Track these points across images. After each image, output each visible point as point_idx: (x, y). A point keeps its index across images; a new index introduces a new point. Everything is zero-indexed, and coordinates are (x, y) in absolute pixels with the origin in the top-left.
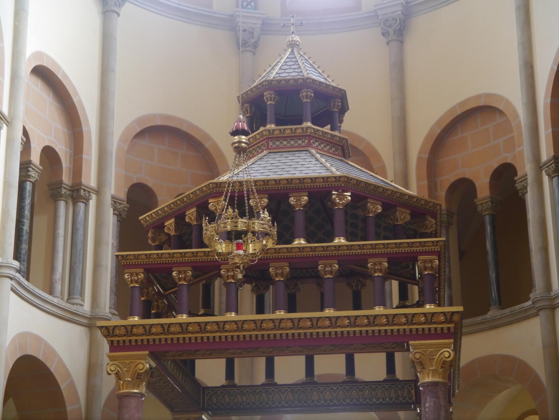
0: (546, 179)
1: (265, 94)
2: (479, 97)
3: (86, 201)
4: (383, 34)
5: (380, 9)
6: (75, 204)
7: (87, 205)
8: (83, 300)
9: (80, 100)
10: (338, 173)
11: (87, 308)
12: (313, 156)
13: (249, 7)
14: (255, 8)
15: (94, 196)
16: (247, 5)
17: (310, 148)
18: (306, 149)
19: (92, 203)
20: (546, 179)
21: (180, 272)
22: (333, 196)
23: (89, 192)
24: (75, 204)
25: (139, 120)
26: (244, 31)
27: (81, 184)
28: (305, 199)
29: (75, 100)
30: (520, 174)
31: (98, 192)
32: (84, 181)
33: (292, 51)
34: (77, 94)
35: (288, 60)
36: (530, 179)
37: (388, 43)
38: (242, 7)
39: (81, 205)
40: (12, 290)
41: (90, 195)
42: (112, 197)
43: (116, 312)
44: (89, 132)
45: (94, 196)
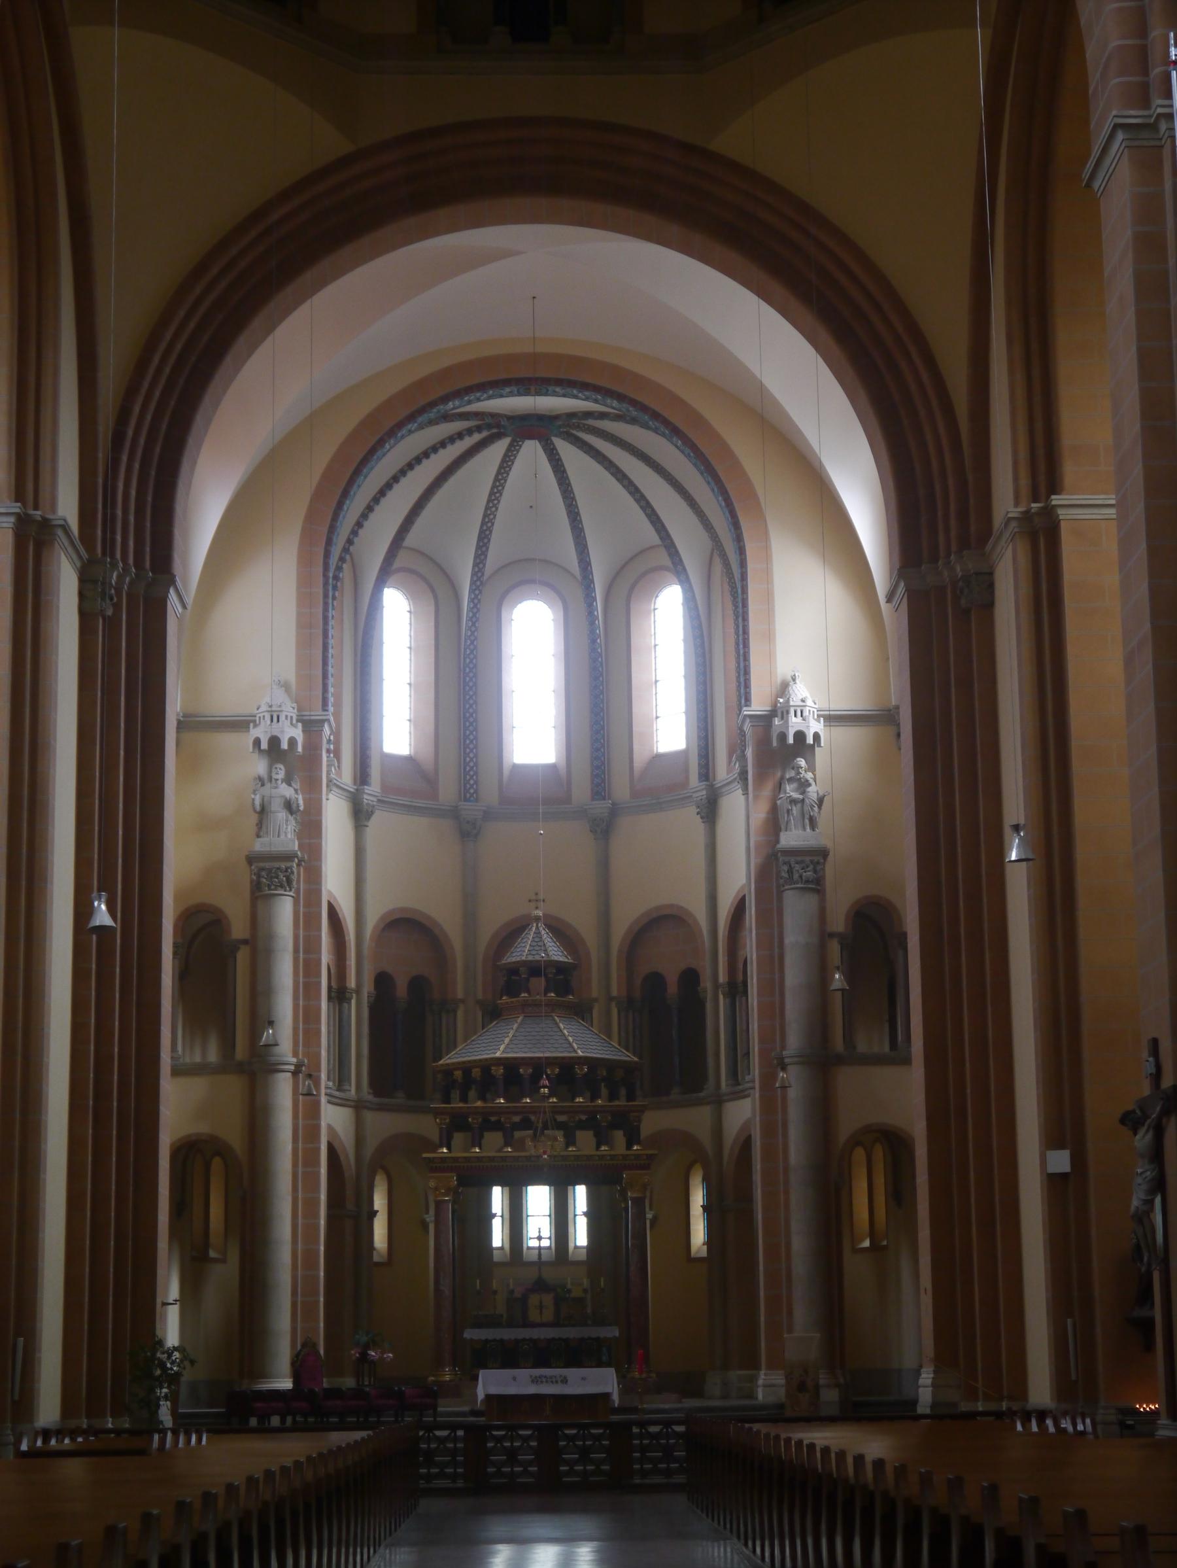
0: (721, 997)
1: (521, 969)
2: (672, 906)
3: (349, 1001)
4: (591, 831)
5: (590, 808)
6: (340, 1004)
7: (350, 1004)
8: (350, 1085)
9: (343, 914)
10: (580, 1053)
11: (353, 1092)
12: (556, 1024)
13: (472, 799)
14: (477, 800)
15: (354, 995)
16: (470, 797)
17: (554, 1014)
18: (550, 1014)
19: (353, 1002)
20: (721, 997)
21: (473, 1119)
22: (576, 1069)
23: (351, 993)
24: (340, 1004)
25: (382, 918)
26: (468, 822)
27: (346, 988)
28: (557, 1071)
29: (340, 916)
30: (702, 985)
31: (358, 991)
32: (348, 985)
33: (537, 925)
34: (341, 910)
35: (535, 944)
36: (709, 996)
37: (595, 839)
38: (466, 800)
39: (346, 1005)
40: (329, 1102)
41: (352, 996)
42: (368, 993)
43: (371, 1091)
44: (350, 939)
45: (354, 995)
